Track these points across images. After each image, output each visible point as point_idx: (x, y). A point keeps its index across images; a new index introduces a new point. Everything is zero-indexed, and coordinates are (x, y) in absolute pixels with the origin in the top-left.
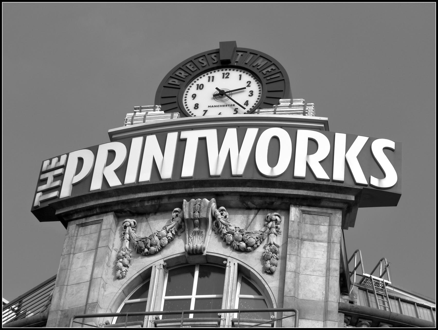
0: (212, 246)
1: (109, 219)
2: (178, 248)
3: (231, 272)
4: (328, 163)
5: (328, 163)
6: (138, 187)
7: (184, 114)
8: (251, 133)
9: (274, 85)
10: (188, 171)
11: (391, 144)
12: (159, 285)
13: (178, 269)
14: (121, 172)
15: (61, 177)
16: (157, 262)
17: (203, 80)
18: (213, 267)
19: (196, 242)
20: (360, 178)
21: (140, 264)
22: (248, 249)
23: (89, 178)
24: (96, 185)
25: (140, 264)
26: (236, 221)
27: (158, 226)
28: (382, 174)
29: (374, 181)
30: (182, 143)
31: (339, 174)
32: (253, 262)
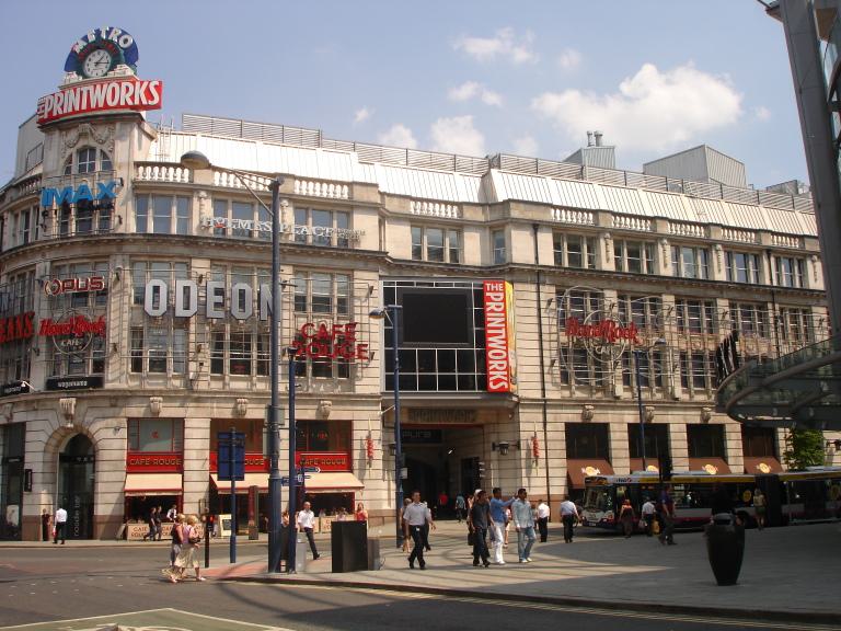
2: (80, 145)
3: (98, 153)
5: (133, 98)
6: (68, 114)
7: (85, 77)
8: (105, 86)
10: (84, 107)
12: (75, 159)
13: (82, 153)
15: (43, 108)
16: (74, 150)
17: (87, 61)
18: (93, 150)
19: (86, 143)
21: (69, 151)
22: (103, 143)
24: (55, 114)
25: (69, 151)
27: (73, 135)
28: (152, 98)
29: (150, 103)
30: (81, 93)
31: (137, 102)
32: (106, 150)
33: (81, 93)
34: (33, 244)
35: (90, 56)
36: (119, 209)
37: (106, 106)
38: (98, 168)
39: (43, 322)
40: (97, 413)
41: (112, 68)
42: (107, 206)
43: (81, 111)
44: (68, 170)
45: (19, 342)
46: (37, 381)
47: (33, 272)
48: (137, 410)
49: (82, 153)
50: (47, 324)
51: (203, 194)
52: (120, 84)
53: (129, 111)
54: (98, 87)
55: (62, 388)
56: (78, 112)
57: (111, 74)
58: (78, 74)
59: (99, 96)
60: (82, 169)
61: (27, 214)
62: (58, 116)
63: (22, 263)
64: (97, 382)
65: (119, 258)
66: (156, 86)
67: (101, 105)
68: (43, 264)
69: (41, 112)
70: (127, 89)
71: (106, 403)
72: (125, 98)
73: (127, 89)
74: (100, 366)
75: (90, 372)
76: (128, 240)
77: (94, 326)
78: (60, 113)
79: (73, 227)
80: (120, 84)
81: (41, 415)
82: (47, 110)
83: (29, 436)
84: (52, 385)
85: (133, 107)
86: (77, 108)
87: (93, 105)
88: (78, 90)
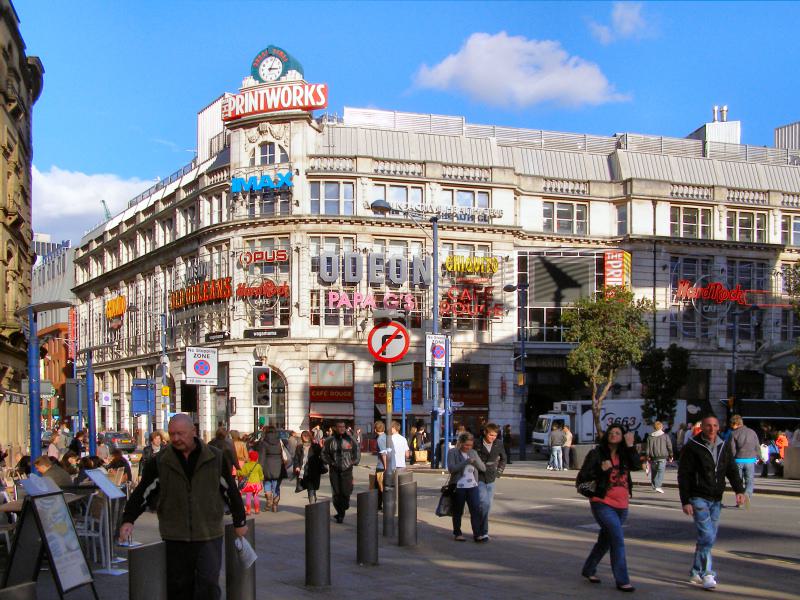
0: (269, 138)
1: (241, 129)
2: (259, 142)
3: (277, 147)
4: (303, 100)
5: (303, 100)
8: (279, 90)
9: (288, 64)
10: (262, 108)
11: (323, 86)
14: (244, 107)
16: (256, 145)
17: (261, 67)
20: (313, 104)
23: (235, 110)
25: (252, 146)
26: (277, 128)
28: (320, 100)
29: (319, 104)
30: (259, 95)
31: (307, 104)
33: (259, 95)
34: (227, 223)
35: (264, 62)
36: (296, 196)
37: (281, 108)
38: (278, 159)
39: (240, 285)
40: (286, 356)
41: (284, 73)
42: (286, 192)
43: (260, 112)
44: (253, 161)
45: (218, 301)
46: (237, 329)
47: (228, 245)
48: (315, 351)
49: (263, 145)
50: (241, 288)
51: (365, 180)
52: (291, 88)
53: (300, 111)
54: (273, 91)
55: (258, 337)
56: (256, 113)
57: (283, 79)
58: (255, 79)
59: (273, 100)
60: (264, 160)
61: (219, 197)
62: (239, 117)
63: (219, 237)
64: (283, 333)
65: (298, 235)
66: (322, 89)
67: (276, 106)
68: (236, 239)
69: (225, 111)
70: (298, 91)
71: (292, 348)
72: (296, 100)
73: (298, 91)
74: (285, 319)
75: (278, 325)
76: (304, 220)
77: (282, 289)
78: (242, 112)
79: (257, 210)
80: (291, 88)
81: (240, 357)
82: (231, 109)
83: (232, 373)
84: (248, 334)
85: (303, 108)
86: (256, 109)
87: (270, 106)
88: (256, 93)
